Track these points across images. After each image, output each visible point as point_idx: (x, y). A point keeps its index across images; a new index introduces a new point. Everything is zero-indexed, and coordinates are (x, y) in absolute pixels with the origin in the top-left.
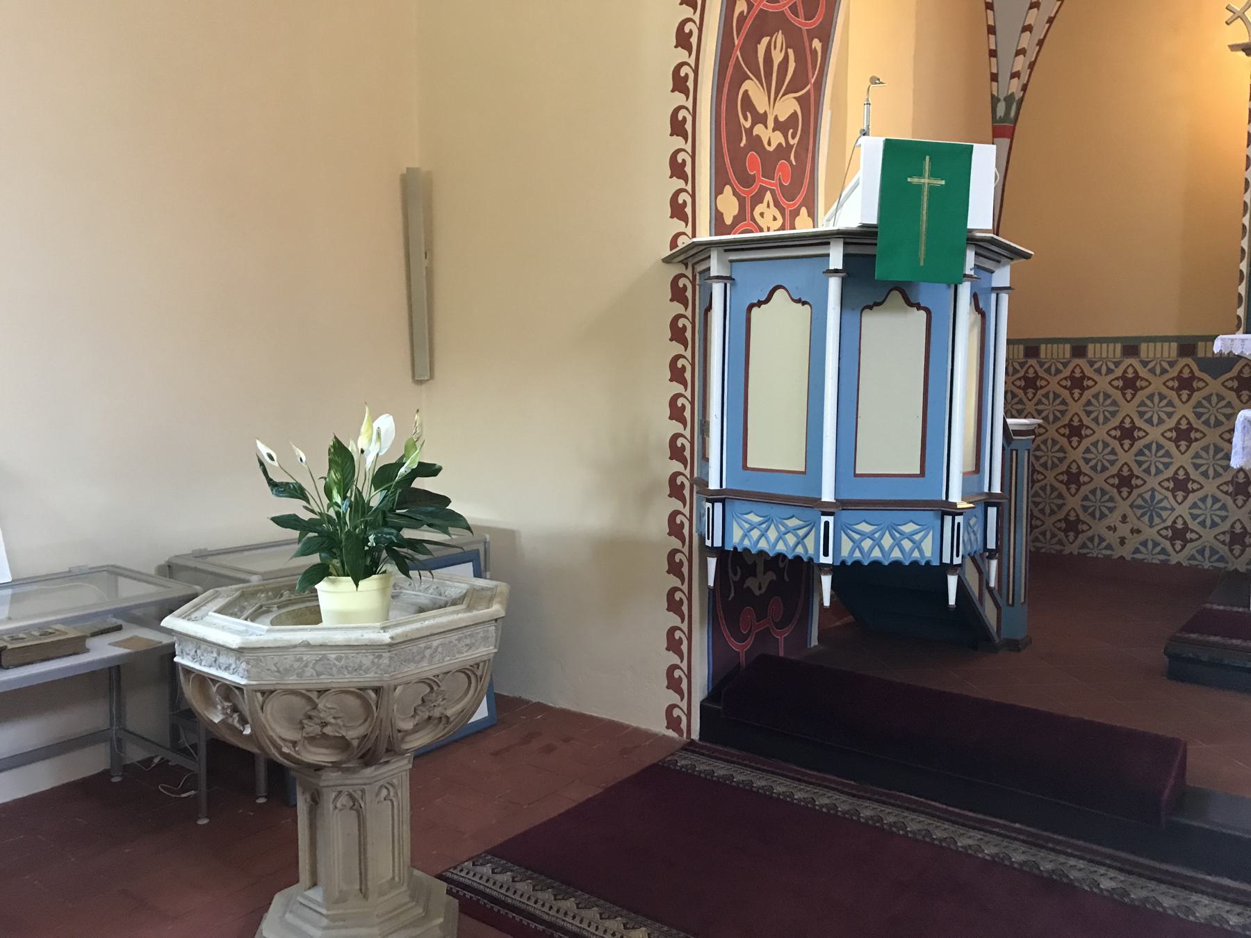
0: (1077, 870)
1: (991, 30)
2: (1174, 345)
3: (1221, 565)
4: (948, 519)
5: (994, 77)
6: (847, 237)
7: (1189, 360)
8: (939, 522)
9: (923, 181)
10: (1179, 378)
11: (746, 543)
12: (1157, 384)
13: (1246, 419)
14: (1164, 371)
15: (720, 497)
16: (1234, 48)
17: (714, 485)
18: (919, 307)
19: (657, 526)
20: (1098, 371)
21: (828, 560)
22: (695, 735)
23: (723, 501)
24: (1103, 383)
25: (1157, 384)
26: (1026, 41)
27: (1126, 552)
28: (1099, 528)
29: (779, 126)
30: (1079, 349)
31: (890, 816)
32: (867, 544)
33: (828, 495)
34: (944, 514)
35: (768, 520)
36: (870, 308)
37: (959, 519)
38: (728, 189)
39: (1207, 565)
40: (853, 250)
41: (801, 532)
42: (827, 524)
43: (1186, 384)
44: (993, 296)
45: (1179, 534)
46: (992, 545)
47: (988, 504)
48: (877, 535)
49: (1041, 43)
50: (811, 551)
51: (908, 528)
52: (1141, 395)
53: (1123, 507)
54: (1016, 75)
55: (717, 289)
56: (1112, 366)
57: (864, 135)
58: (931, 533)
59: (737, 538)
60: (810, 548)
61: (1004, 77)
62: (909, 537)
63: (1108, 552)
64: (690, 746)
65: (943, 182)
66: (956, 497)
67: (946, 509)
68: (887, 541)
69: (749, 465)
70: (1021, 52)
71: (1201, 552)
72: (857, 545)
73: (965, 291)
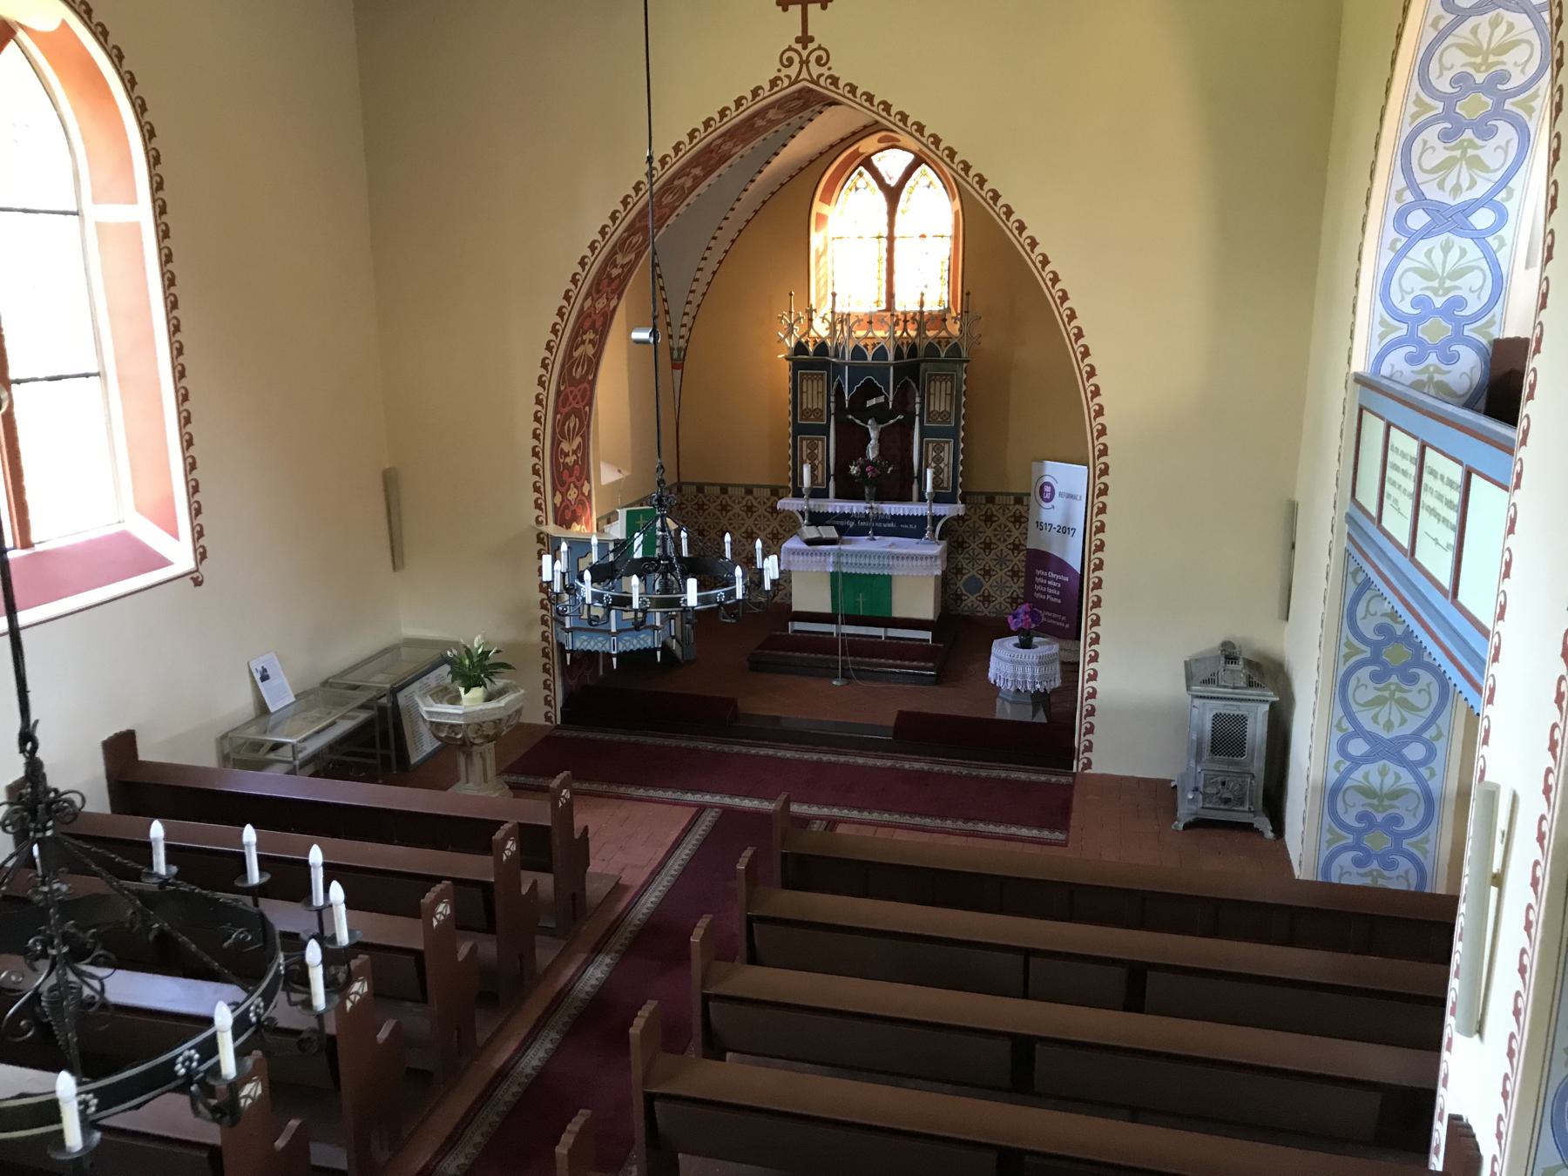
0: (701, 745)
2: (769, 490)
5: (670, 337)
15: (571, 630)
19: (535, 636)
20: (734, 502)
22: (559, 723)
24: (737, 509)
25: (762, 511)
26: (686, 320)
30: (724, 489)
31: (641, 739)
32: (628, 644)
33: (614, 630)
35: (592, 638)
38: (558, 493)
46: (673, 634)
54: (682, 337)
59: (578, 645)
60: (607, 647)
61: (676, 337)
62: (643, 639)
64: (557, 727)
66: (658, 624)
72: (625, 645)
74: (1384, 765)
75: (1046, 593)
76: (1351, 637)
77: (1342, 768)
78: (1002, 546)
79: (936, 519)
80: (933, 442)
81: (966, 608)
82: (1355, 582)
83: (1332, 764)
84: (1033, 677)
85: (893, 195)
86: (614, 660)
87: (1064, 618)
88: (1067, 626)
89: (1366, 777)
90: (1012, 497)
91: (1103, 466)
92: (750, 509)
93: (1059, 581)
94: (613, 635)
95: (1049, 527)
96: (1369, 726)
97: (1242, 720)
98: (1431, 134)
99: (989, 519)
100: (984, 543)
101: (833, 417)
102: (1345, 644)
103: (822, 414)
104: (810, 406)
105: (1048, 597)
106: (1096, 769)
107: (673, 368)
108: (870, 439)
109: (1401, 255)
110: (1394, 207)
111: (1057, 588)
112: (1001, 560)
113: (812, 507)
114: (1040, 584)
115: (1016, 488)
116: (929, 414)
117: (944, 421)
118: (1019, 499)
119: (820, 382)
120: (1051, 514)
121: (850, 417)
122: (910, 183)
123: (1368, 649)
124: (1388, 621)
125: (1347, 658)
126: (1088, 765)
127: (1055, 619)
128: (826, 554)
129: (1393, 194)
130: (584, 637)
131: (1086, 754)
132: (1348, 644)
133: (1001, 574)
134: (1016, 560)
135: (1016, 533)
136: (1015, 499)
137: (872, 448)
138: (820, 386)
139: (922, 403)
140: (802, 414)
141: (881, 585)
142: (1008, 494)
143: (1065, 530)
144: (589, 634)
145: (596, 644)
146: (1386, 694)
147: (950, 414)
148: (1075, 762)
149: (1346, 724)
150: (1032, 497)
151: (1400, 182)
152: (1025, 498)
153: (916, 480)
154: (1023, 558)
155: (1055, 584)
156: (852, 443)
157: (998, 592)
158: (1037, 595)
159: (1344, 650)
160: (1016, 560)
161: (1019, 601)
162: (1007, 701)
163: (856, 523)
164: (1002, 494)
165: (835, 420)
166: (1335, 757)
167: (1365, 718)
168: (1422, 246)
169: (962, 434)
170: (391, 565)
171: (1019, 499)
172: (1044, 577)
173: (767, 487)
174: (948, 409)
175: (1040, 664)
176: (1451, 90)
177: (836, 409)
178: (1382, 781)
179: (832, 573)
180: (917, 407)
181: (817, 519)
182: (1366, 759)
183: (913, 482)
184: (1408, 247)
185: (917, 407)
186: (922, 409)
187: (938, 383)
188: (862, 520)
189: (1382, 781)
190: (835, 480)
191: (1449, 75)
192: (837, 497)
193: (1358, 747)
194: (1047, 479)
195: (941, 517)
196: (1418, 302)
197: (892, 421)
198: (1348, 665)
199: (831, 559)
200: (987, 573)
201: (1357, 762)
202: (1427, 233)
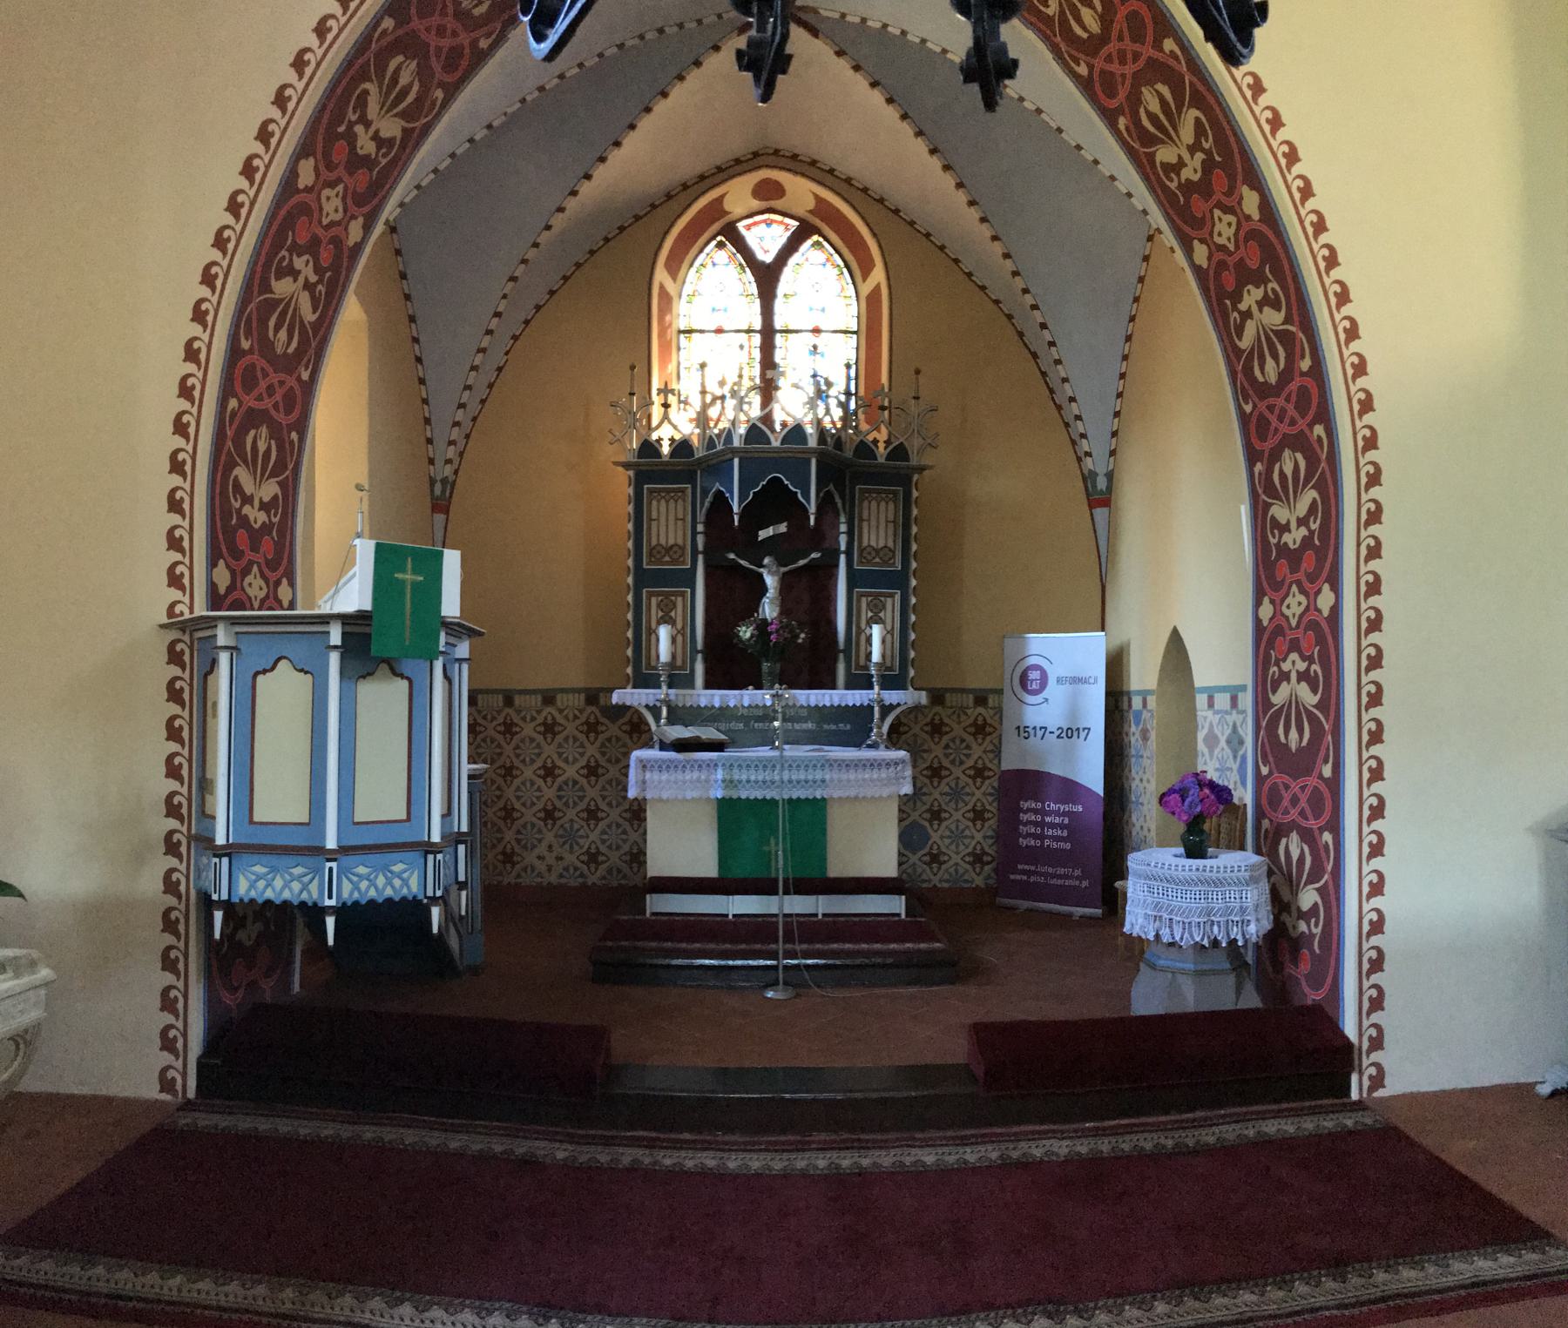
3: (623, 882)
4: (430, 857)
6: (344, 619)
7: (593, 708)
8: (422, 860)
9: (407, 576)
11: (253, 894)
13: (637, 758)
15: (229, 851)
16: (616, 464)
17: (220, 840)
18: (402, 676)
19: (149, 883)
20: (524, 719)
21: (332, 903)
23: (229, 855)
24: (528, 730)
25: (571, 729)
27: (553, 879)
28: (530, 858)
29: (264, 507)
32: (364, 885)
34: (427, 852)
35: (274, 870)
36: (364, 677)
37: (439, 856)
39: (615, 884)
40: (349, 629)
41: (306, 879)
42: (331, 870)
43: (592, 728)
44: (457, 665)
45: (593, 858)
46: (462, 878)
47: (459, 842)
48: (372, 876)
50: (315, 895)
51: (398, 868)
52: (559, 738)
53: (549, 837)
55: (224, 658)
56: (535, 714)
57: (358, 537)
58: (416, 873)
59: (243, 889)
60: (313, 892)
63: (539, 880)
65: (422, 578)
67: (428, 848)
68: (381, 881)
69: (256, 819)
71: (610, 871)
73: (438, 666)
75: (1042, 837)
78: (957, 772)
79: (886, 710)
85: (767, 277)
86: (330, 922)
87: (1078, 872)
88: (1085, 884)
92: (550, 729)
93: (1065, 814)
94: (331, 856)
95: (1040, 733)
99: (937, 729)
101: (700, 558)
103: (683, 555)
104: (663, 542)
105: (1047, 842)
106: (1392, 1087)
107: (433, 511)
108: (763, 589)
111: (1061, 826)
113: (672, 697)
114: (1029, 822)
115: (977, 680)
116: (861, 551)
117: (885, 563)
119: (680, 502)
120: (1045, 711)
121: (732, 556)
122: (792, 261)
126: (1378, 1081)
127: (1060, 877)
128: (713, 765)
130: (259, 869)
131: (1375, 1057)
133: (957, 816)
134: (978, 794)
135: (977, 751)
137: (771, 602)
138: (682, 508)
139: (850, 533)
140: (650, 554)
142: (963, 691)
143: (1070, 733)
144: (273, 860)
145: (286, 885)
148: (1354, 1078)
153: (841, 656)
154: (990, 790)
155: (1057, 820)
157: (953, 847)
158: (1023, 842)
161: (986, 858)
162: (1183, 972)
164: (954, 690)
169: (914, 583)
171: (981, 699)
172: (1036, 811)
174: (890, 544)
177: (706, 545)
180: (843, 540)
181: (677, 715)
183: (835, 660)
185: (843, 540)
186: (850, 544)
187: (874, 504)
190: (705, 660)
192: (708, 685)
194: (1032, 661)
195: (892, 707)
197: (802, 562)
199: (720, 774)
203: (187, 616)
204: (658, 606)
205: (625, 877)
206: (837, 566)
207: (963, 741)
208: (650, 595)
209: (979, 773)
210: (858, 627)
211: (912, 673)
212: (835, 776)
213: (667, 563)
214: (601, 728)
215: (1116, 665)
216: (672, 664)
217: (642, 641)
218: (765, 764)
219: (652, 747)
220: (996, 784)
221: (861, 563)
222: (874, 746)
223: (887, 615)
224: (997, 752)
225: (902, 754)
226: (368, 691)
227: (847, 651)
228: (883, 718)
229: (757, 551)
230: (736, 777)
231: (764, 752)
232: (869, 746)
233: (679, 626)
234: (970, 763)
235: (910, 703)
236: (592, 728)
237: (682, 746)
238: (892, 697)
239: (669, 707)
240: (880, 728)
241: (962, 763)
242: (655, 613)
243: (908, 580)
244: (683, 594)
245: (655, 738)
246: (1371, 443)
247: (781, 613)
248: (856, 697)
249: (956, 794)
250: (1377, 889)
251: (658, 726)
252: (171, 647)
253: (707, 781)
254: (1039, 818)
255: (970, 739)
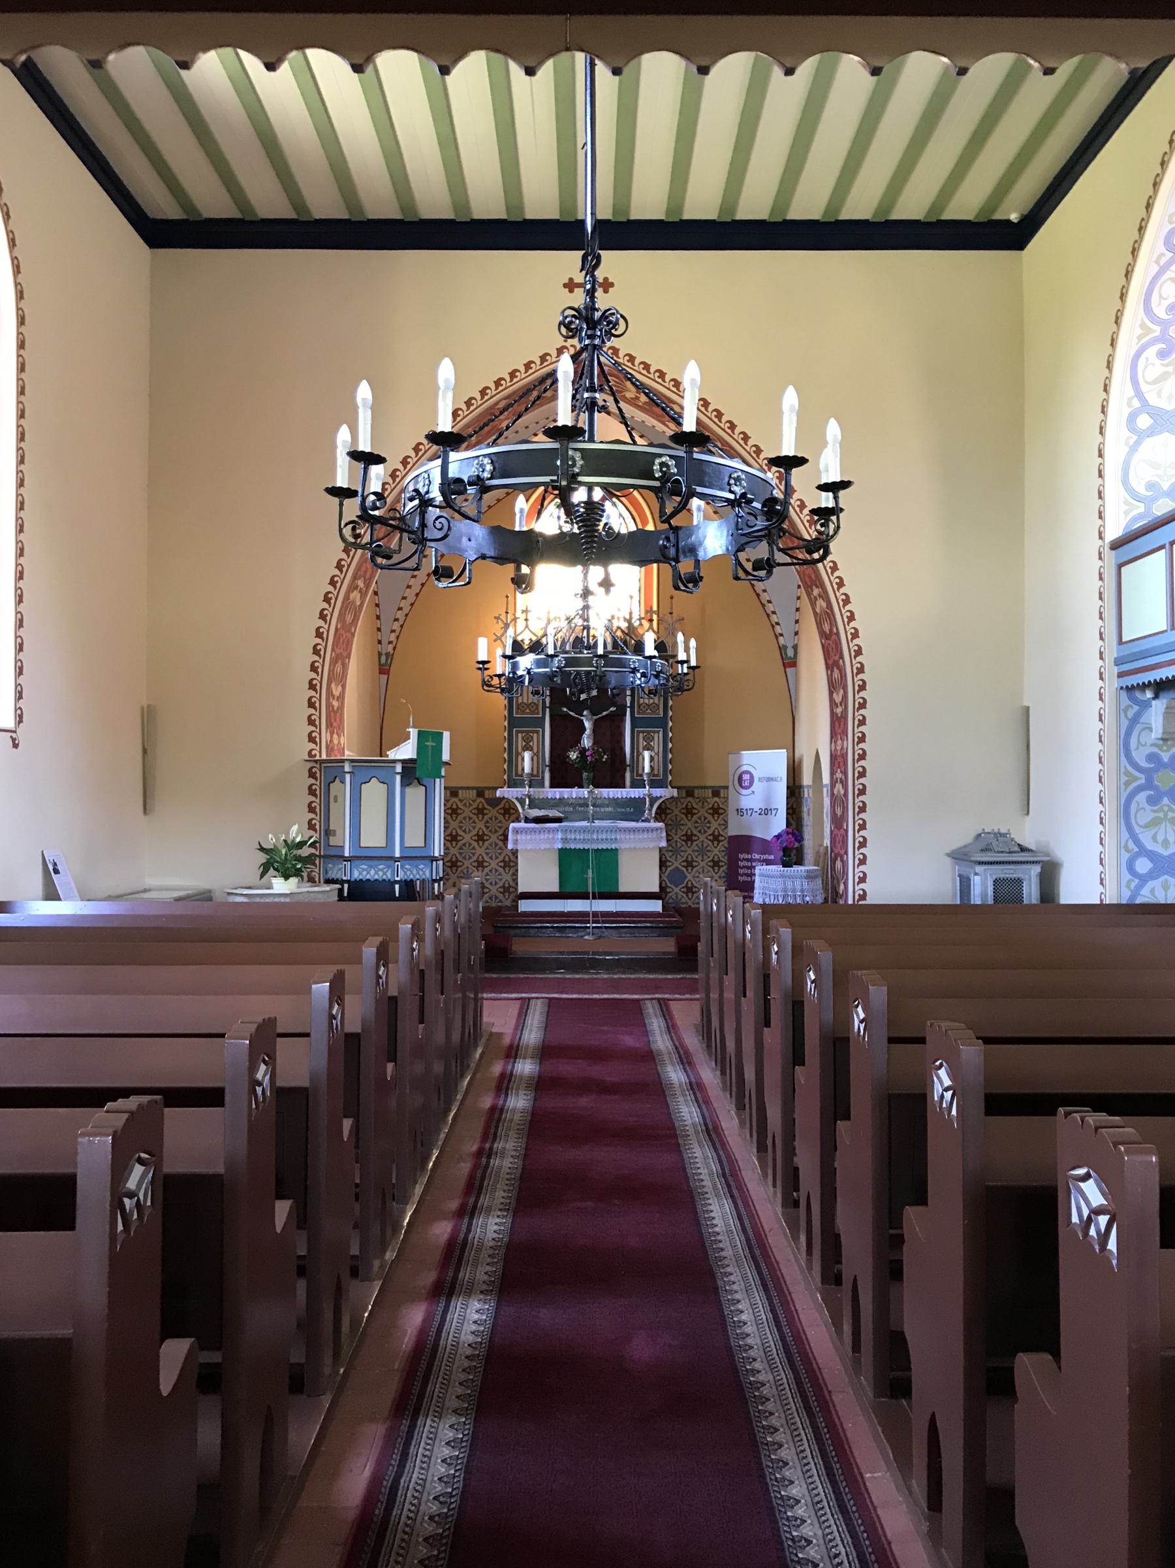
1: (378, 617)
2: (475, 791)
3: (500, 904)
5: (380, 642)
6: (404, 761)
10: (477, 808)
11: (361, 877)
12: (467, 812)
14: (470, 805)
25: (467, 812)
26: (396, 626)
35: (371, 867)
39: (494, 905)
43: (480, 811)
49: (402, 626)
51: (421, 866)
52: (460, 817)
54: (390, 643)
55: (348, 777)
59: (356, 875)
62: (422, 870)
67: (434, 859)
70: (393, 631)
74: (1166, 880)
76: (1130, 768)
77: (1133, 885)
78: (702, 837)
79: (653, 800)
80: (643, 732)
81: (671, 901)
82: (1126, 717)
83: (1124, 883)
84: (802, 891)
86: (397, 887)
89: (1152, 891)
90: (710, 791)
91: (861, 683)
94: (396, 860)
95: (749, 812)
96: (1150, 846)
97: (1018, 882)
98: (1152, 352)
99: (689, 812)
100: (686, 835)
101: (548, 710)
102: (1125, 773)
103: (537, 709)
104: (525, 701)
108: (584, 729)
109: (1134, 449)
110: (1127, 411)
112: (703, 851)
114: (744, 867)
116: (639, 706)
117: (653, 712)
118: (716, 793)
120: (751, 800)
121: (565, 709)
123: (1143, 776)
124: (1156, 750)
125: (1127, 784)
128: (555, 830)
129: (1126, 401)
132: (1127, 773)
134: (716, 851)
135: (714, 825)
136: (713, 792)
137: (588, 738)
140: (518, 708)
141: (608, 859)
142: (706, 788)
143: (767, 812)
144: (370, 863)
146: (1161, 815)
147: (658, 706)
149: (1131, 845)
150: (731, 788)
151: (1130, 392)
152: (722, 791)
156: (565, 733)
159: (1124, 779)
160: (716, 851)
163: (574, 808)
165: (551, 716)
166: (1127, 876)
167: (1145, 838)
168: (1148, 442)
169: (670, 724)
170: (141, 808)
171: (716, 793)
172: (748, 860)
173: (473, 788)
175: (808, 877)
176: (1166, 317)
177: (550, 703)
178: (1166, 895)
179: (560, 850)
180: (628, 699)
182: (1151, 876)
183: (625, 770)
184: (1138, 443)
185: (628, 699)
186: (632, 702)
188: (581, 805)
189: (1166, 895)
190: (551, 771)
191: (1165, 304)
192: (552, 786)
193: (1143, 865)
194: (745, 768)
195: (657, 798)
196: (1151, 486)
197: (605, 713)
198: (1129, 790)
199: (560, 836)
200: (689, 864)
201: (1144, 879)
202: (1151, 432)
203: (318, 758)
204: (522, 738)
205: (501, 901)
206: (625, 715)
207: (705, 818)
208: (518, 732)
209: (716, 838)
210: (638, 751)
211: (670, 778)
212: (623, 837)
213: (528, 713)
214: (485, 811)
215: (794, 770)
216: (531, 775)
217: (513, 760)
218: (584, 830)
219: (520, 822)
220: (726, 845)
221: (639, 713)
222: (647, 820)
223: (654, 744)
224: (725, 824)
225: (661, 825)
226: (409, 790)
227: (632, 766)
228: (651, 805)
229: (579, 707)
230: (569, 837)
231: (585, 823)
232: (643, 821)
233: (535, 751)
234: (710, 832)
235: (668, 796)
236: (480, 811)
237: (538, 820)
238: (657, 792)
239: (529, 798)
240: (650, 810)
241: (705, 832)
242: (521, 743)
243: (667, 723)
244: (537, 732)
245: (522, 816)
246: (861, 670)
247: (594, 744)
248: (636, 793)
249: (703, 851)
250: (863, 880)
251: (524, 810)
252: (310, 770)
253: (553, 838)
254: (749, 864)
255: (710, 817)
